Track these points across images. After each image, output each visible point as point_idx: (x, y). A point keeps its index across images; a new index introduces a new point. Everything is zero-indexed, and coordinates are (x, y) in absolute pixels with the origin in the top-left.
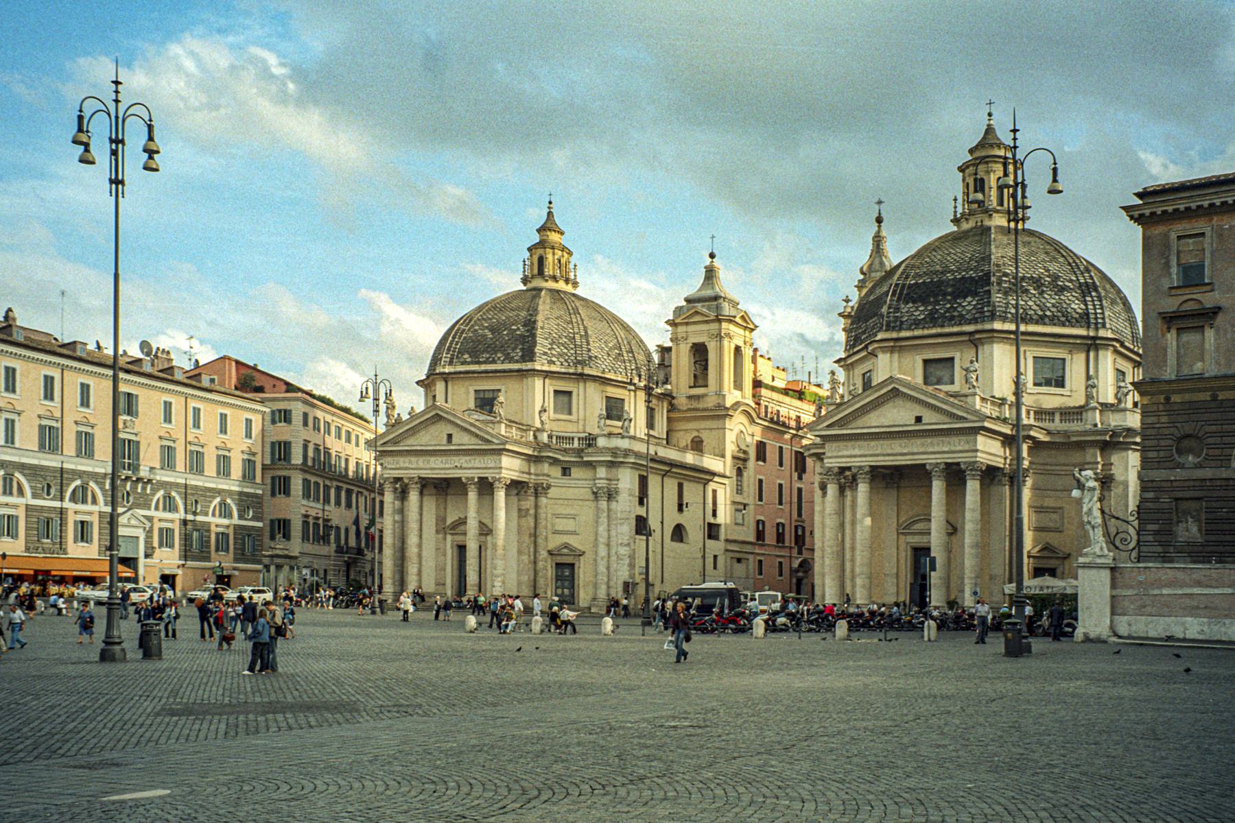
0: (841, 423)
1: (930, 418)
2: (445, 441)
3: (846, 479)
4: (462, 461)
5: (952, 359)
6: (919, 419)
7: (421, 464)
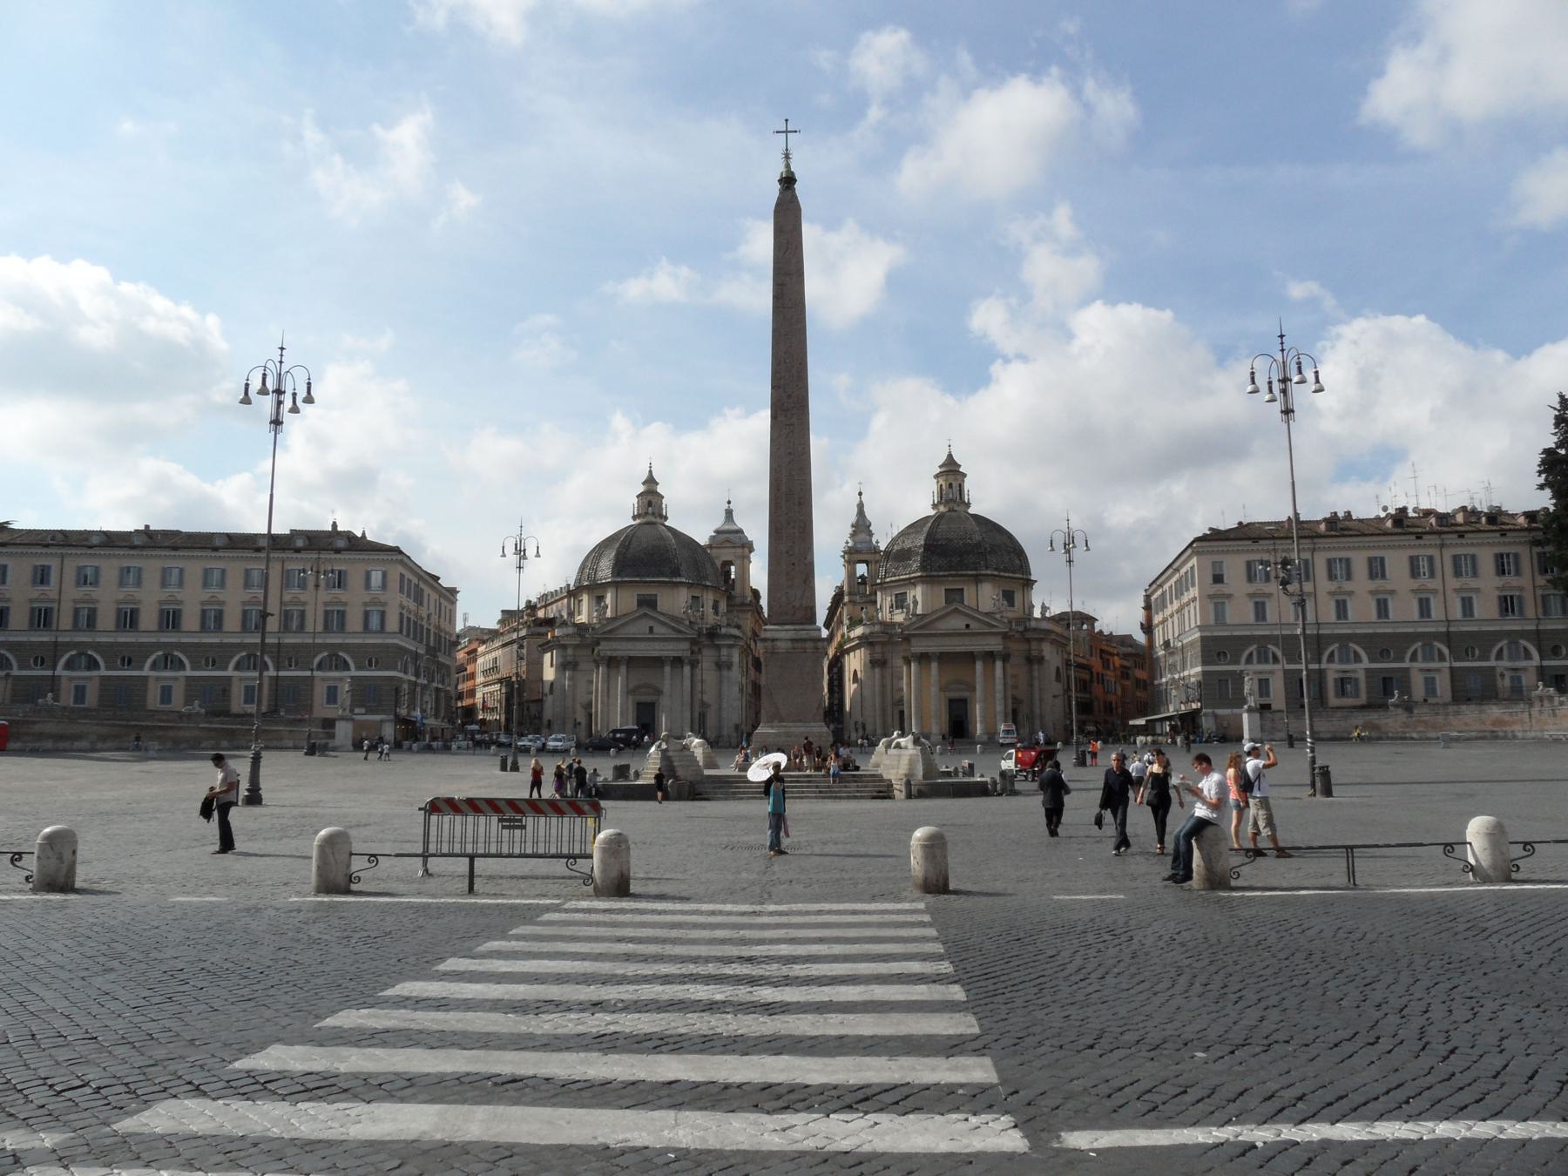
0: (921, 628)
1: (973, 625)
4: (657, 645)
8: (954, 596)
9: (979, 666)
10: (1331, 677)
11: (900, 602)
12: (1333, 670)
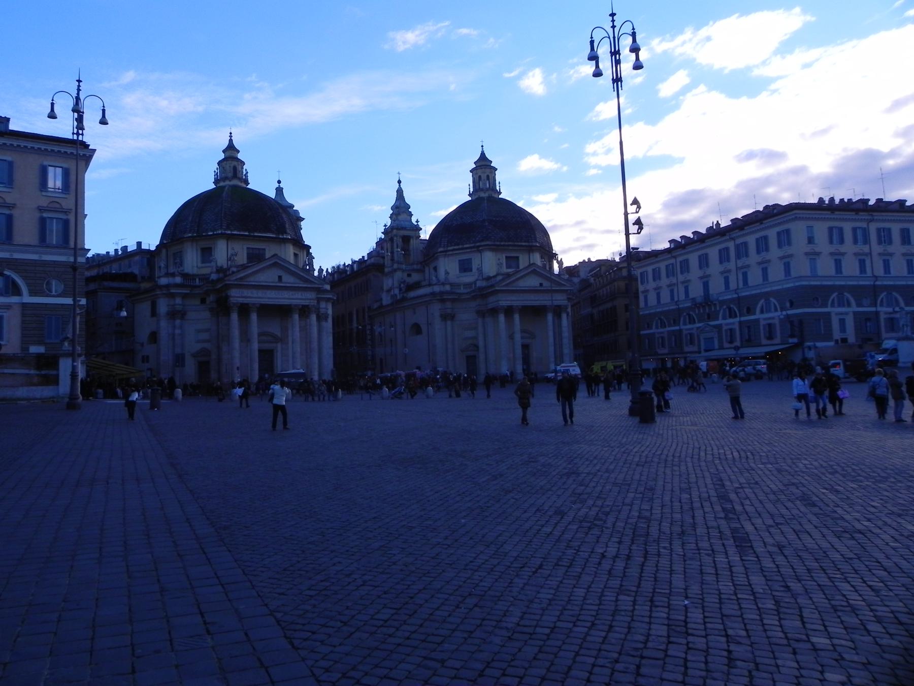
0: (507, 285)
2: (277, 280)
3: (509, 311)
5: (518, 258)
6: (541, 285)
7: (260, 295)
8: (512, 261)
9: (550, 317)
10: (882, 317)
11: (465, 267)
12: (884, 311)
